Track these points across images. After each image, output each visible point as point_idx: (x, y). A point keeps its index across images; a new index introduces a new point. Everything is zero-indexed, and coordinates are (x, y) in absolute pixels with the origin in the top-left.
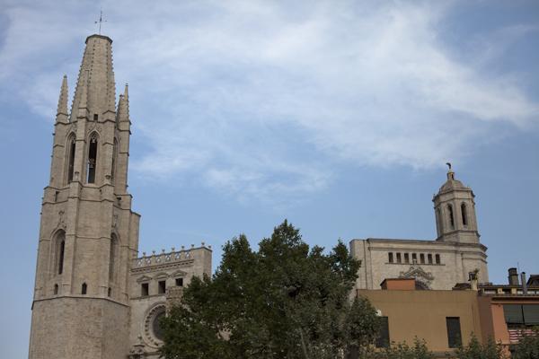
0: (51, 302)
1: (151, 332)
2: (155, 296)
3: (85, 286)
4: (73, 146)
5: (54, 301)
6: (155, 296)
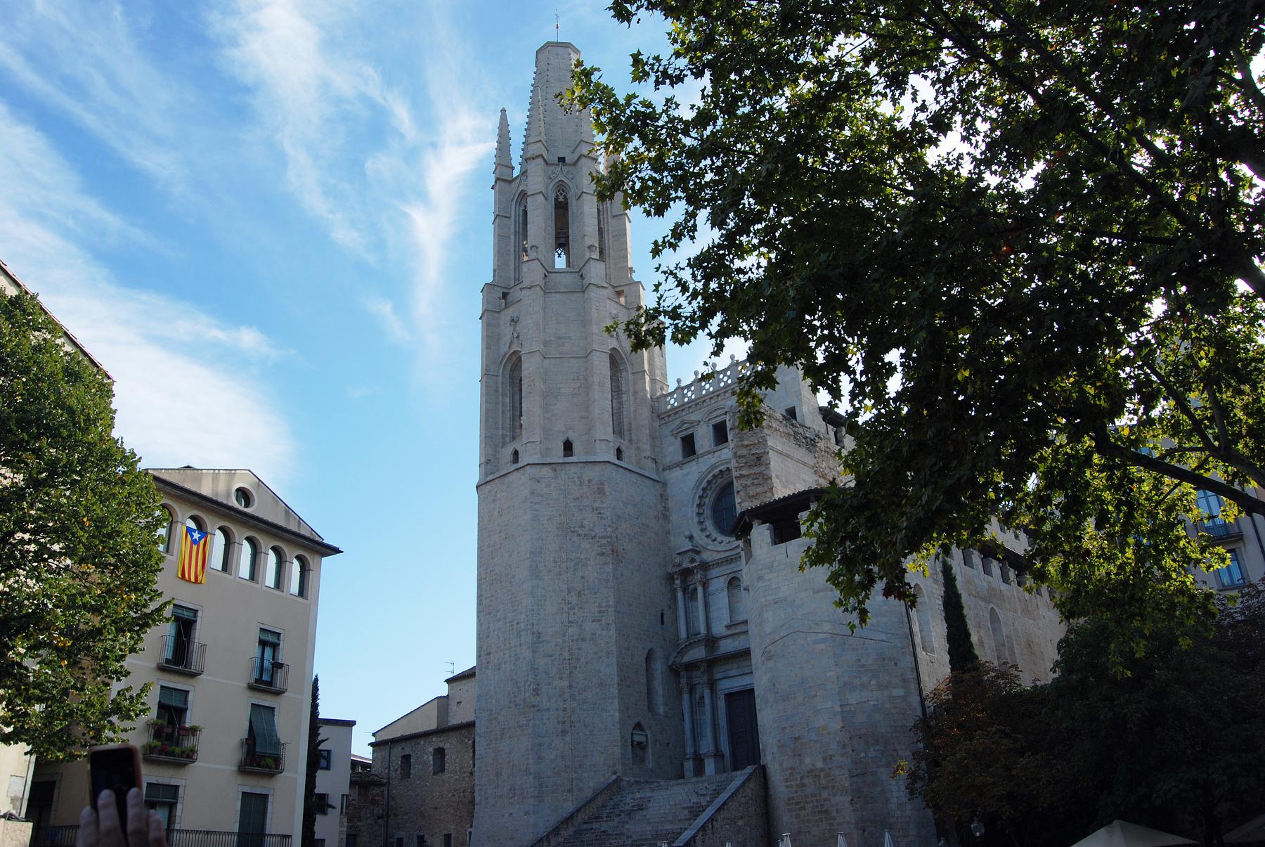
0: (506, 480)
1: (709, 524)
2: (708, 453)
3: (568, 447)
4: (525, 212)
5: (511, 478)
6: (708, 453)
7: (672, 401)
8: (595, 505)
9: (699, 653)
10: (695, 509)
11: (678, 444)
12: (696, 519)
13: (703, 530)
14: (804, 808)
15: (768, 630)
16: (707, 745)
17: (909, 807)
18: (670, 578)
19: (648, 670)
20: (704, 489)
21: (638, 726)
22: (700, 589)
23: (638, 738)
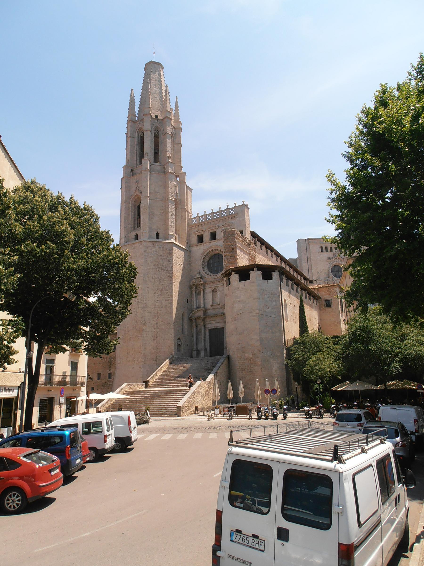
0: (134, 246)
1: (206, 268)
5: (136, 245)
7: (195, 221)
8: (168, 258)
9: (200, 314)
10: (202, 263)
12: (201, 266)
13: (203, 270)
14: (244, 370)
15: (235, 311)
16: (201, 346)
17: (278, 371)
19: (183, 319)
21: (179, 339)
22: (202, 292)
23: (179, 343)
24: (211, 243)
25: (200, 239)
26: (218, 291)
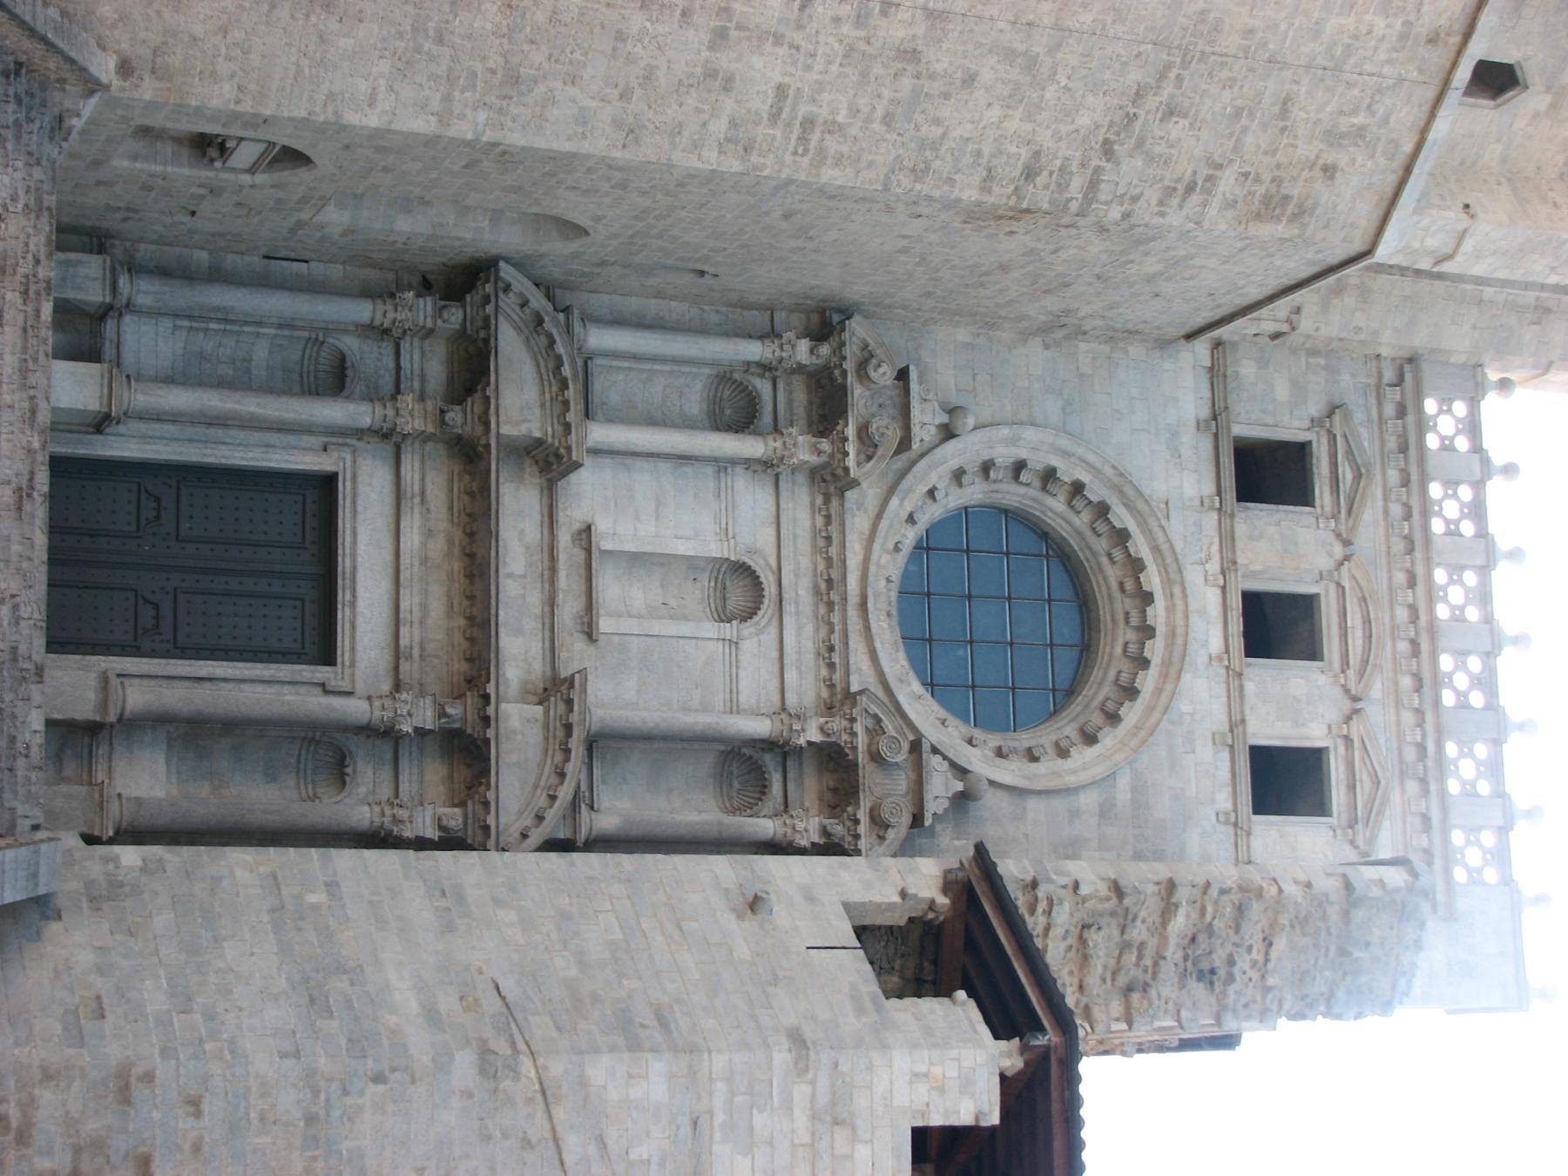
2: (1229, 565)
8: (1227, 183)
9: (519, 405)
10: (1038, 461)
11: (1290, 429)
12: (1004, 455)
15: (600, 1071)
18: (826, 322)
20: (1102, 510)
21: (292, 157)
23: (245, 155)
24: (1212, 597)
25: (1267, 473)
26: (729, 630)
